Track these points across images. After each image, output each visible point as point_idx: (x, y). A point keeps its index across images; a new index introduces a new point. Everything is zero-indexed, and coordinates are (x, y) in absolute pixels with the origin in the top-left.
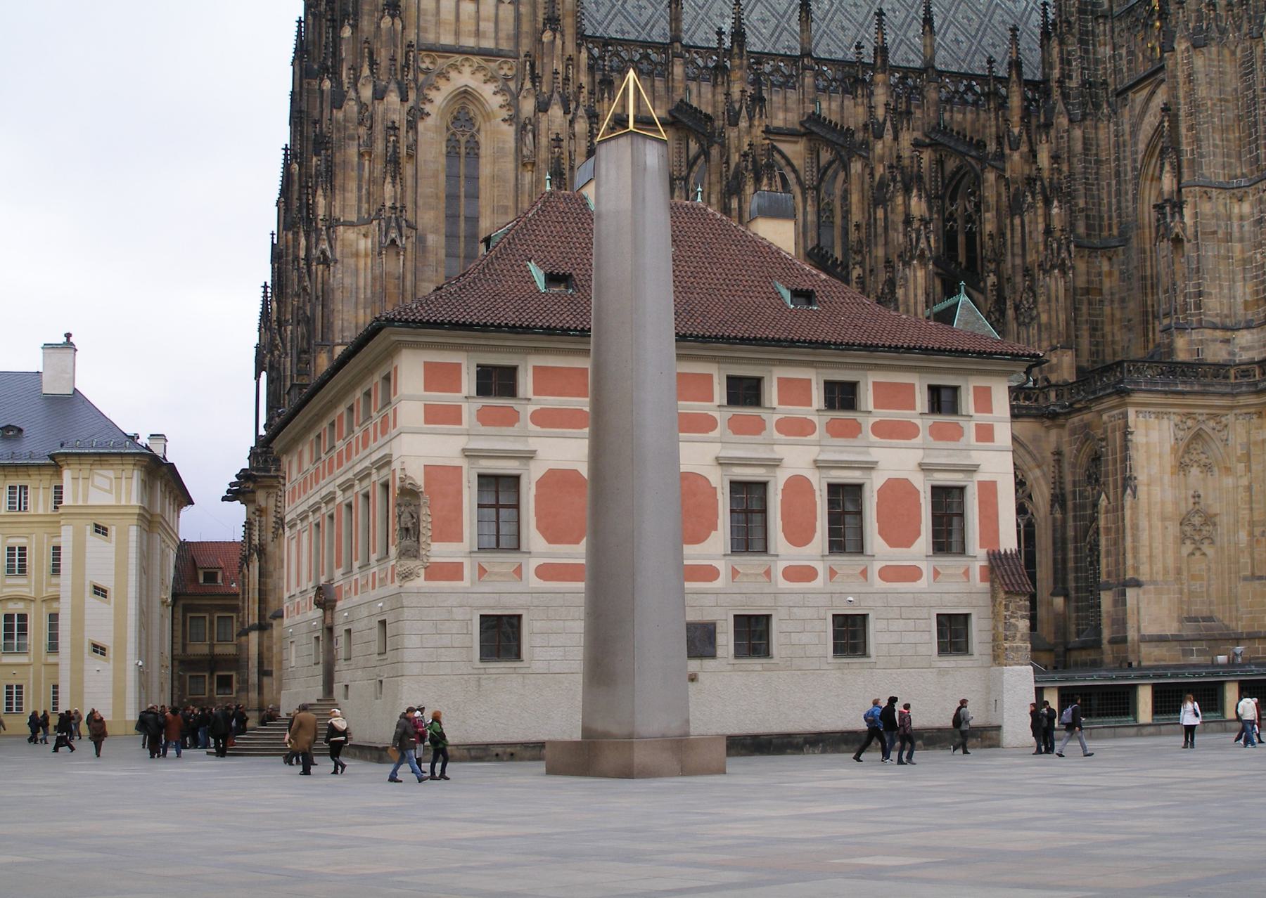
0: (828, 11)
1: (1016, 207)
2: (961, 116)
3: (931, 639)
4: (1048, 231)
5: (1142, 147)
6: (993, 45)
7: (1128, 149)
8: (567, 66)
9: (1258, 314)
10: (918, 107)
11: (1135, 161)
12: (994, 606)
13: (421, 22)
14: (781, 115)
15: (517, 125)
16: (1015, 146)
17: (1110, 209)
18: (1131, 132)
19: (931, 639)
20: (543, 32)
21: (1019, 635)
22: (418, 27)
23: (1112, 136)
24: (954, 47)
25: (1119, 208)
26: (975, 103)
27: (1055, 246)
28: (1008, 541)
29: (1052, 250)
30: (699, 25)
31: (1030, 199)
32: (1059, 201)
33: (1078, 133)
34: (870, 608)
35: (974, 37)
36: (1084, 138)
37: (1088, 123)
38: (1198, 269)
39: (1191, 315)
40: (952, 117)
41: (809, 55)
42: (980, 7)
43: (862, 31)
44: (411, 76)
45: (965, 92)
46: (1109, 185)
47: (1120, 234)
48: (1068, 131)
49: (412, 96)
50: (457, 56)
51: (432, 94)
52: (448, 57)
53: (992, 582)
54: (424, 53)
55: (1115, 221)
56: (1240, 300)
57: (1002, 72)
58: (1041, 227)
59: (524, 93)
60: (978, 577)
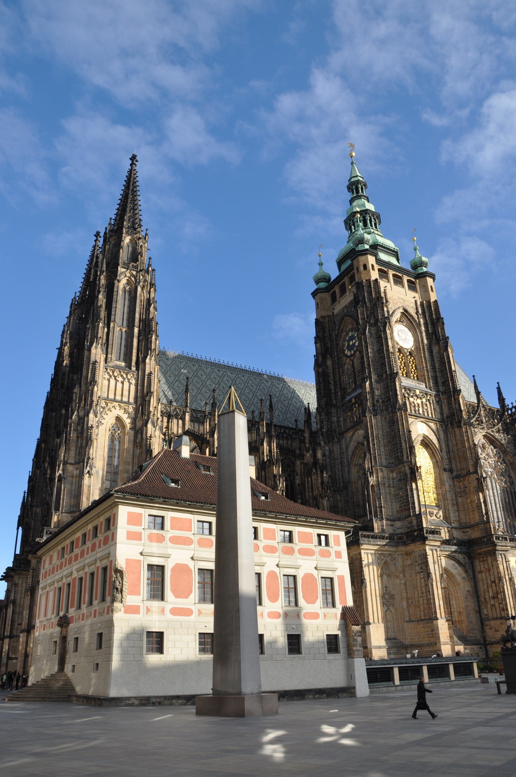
1: (309, 474)
2: (282, 442)
3: (324, 645)
4: (322, 483)
5: (350, 453)
6: (291, 418)
7: (345, 454)
8: (154, 411)
9: (403, 515)
11: (348, 459)
15: (135, 431)
16: (308, 451)
18: (346, 448)
19: (324, 645)
20: (147, 396)
25: (342, 476)
26: (287, 437)
27: (326, 488)
28: (350, 603)
29: (325, 489)
30: (193, 402)
31: (314, 471)
32: (326, 472)
33: (327, 448)
35: (284, 414)
36: (329, 450)
37: (330, 444)
42: (285, 404)
43: (248, 409)
45: (284, 433)
46: (338, 467)
48: (324, 447)
49: (99, 415)
50: (115, 403)
51: (105, 416)
52: (112, 403)
54: (103, 401)
55: (341, 481)
56: (395, 510)
57: (301, 426)
58: (320, 481)
59: (138, 419)
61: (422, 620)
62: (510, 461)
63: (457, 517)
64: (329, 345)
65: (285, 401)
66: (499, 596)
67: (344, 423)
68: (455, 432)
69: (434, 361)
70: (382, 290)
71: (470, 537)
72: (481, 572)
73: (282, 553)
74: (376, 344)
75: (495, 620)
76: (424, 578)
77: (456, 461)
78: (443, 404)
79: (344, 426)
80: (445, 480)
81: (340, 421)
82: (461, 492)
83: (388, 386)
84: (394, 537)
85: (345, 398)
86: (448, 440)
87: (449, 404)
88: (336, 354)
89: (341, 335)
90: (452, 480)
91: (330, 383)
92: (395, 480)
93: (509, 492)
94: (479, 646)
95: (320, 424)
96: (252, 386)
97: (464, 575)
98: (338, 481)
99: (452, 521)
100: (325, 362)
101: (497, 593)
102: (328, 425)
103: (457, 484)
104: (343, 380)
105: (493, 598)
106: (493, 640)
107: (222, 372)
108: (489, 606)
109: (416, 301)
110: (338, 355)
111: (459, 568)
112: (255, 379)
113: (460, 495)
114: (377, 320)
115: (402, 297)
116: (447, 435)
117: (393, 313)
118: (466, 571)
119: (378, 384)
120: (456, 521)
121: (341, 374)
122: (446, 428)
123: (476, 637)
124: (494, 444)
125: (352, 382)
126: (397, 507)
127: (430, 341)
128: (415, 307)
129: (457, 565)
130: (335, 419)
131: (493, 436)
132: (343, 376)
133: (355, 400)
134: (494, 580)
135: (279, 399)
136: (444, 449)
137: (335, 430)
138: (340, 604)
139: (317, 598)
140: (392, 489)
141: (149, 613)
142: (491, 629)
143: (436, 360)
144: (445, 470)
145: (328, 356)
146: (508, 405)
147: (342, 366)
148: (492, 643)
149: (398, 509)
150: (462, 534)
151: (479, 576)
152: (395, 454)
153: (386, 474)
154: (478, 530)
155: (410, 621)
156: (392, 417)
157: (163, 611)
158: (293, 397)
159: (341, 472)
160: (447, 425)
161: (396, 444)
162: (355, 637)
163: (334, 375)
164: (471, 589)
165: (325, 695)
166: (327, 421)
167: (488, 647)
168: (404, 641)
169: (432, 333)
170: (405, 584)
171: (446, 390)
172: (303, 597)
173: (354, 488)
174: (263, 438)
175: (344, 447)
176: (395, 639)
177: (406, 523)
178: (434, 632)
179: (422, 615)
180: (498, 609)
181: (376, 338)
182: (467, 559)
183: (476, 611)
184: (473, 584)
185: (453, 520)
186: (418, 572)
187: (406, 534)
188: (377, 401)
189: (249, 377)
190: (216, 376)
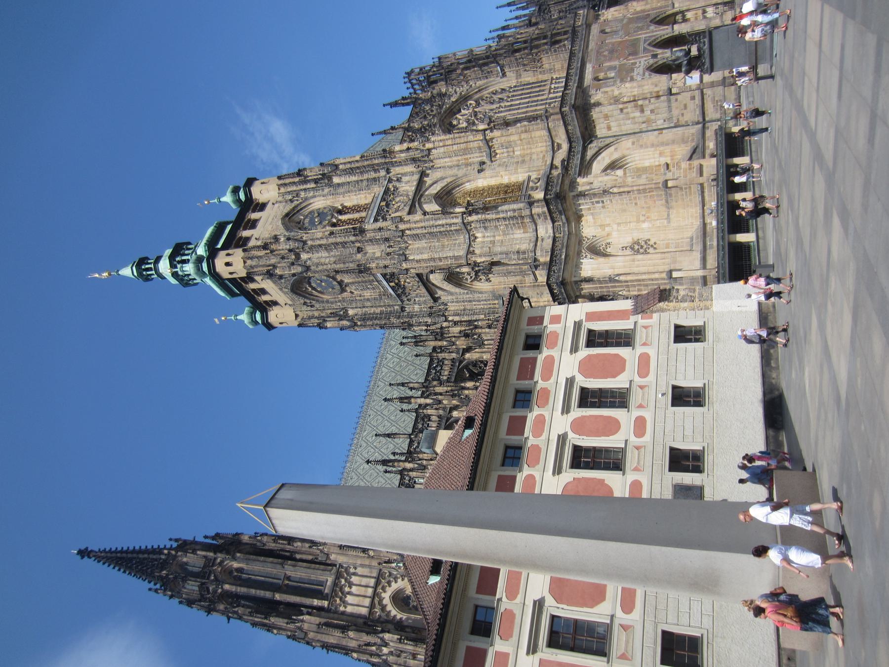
0: (396, 427)
11: (464, 293)
12: (669, 310)
17: (485, 304)
23: (453, 304)
24: (418, 375)
25: (485, 300)
34: (667, 383)
37: (446, 314)
38: (507, 254)
39: (528, 256)
40: (446, 375)
41: (410, 435)
46: (475, 305)
47: (498, 299)
53: (652, 312)
56: (523, 235)
61: (667, 202)
62: (476, 92)
64: (330, 311)
65: (401, 366)
66: (640, 103)
67: (421, 296)
68: (434, 159)
69: (348, 182)
71: (564, 141)
72: (609, 128)
73: (546, 407)
74: (320, 255)
75: (671, 109)
76: (611, 201)
77: (470, 158)
78: (401, 172)
79: (424, 296)
81: (418, 301)
82: (508, 152)
83: (371, 240)
84: (557, 238)
85: (391, 294)
87: (399, 164)
88: (339, 304)
89: (317, 296)
91: (374, 313)
92: (486, 235)
95: (422, 326)
96: (382, 405)
97: (612, 149)
98: (492, 306)
101: (636, 106)
102: (423, 316)
103: (498, 156)
104: (370, 296)
105: (642, 111)
106: (698, 112)
107: (363, 442)
108: (653, 117)
110: (340, 301)
111: (603, 155)
112: (373, 401)
113: (512, 154)
114: (290, 250)
115: (270, 220)
116: (438, 168)
118: (607, 146)
119: (367, 253)
121: (362, 298)
122: (430, 169)
123: (693, 135)
124: (455, 110)
125: (370, 284)
126: (520, 233)
127: (325, 186)
128: (284, 204)
129: (599, 158)
130: (417, 308)
131: (445, 112)
132: (364, 296)
133: (392, 282)
134: (619, 111)
135: (399, 373)
136: (455, 171)
137: (430, 308)
138: (628, 319)
139: (617, 355)
140: (497, 238)
141: (629, 655)
142: (683, 115)
143: (348, 180)
144: (480, 171)
145: (342, 313)
146: (410, 93)
147: (352, 297)
149: (522, 231)
150: (560, 151)
151: (615, 130)
152: (453, 234)
153: (478, 246)
154: (555, 131)
155: (668, 218)
156: (407, 236)
157: (625, 628)
158: (398, 355)
159: (480, 302)
160: (426, 167)
161: (440, 232)
163: (364, 307)
164: (630, 141)
166: (418, 318)
168: (695, 227)
170: (619, 224)
171: (384, 168)
172: (614, 376)
173: (500, 286)
174: (432, 401)
175: (450, 297)
176: (692, 238)
177: (539, 222)
178: (683, 187)
179: (660, 202)
180: (657, 105)
181: (313, 254)
183: (659, 134)
184: (624, 138)
185: (543, 162)
186: (603, 207)
187: (553, 221)
188: (388, 254)
189: (371, 409)
190: (367, 451)
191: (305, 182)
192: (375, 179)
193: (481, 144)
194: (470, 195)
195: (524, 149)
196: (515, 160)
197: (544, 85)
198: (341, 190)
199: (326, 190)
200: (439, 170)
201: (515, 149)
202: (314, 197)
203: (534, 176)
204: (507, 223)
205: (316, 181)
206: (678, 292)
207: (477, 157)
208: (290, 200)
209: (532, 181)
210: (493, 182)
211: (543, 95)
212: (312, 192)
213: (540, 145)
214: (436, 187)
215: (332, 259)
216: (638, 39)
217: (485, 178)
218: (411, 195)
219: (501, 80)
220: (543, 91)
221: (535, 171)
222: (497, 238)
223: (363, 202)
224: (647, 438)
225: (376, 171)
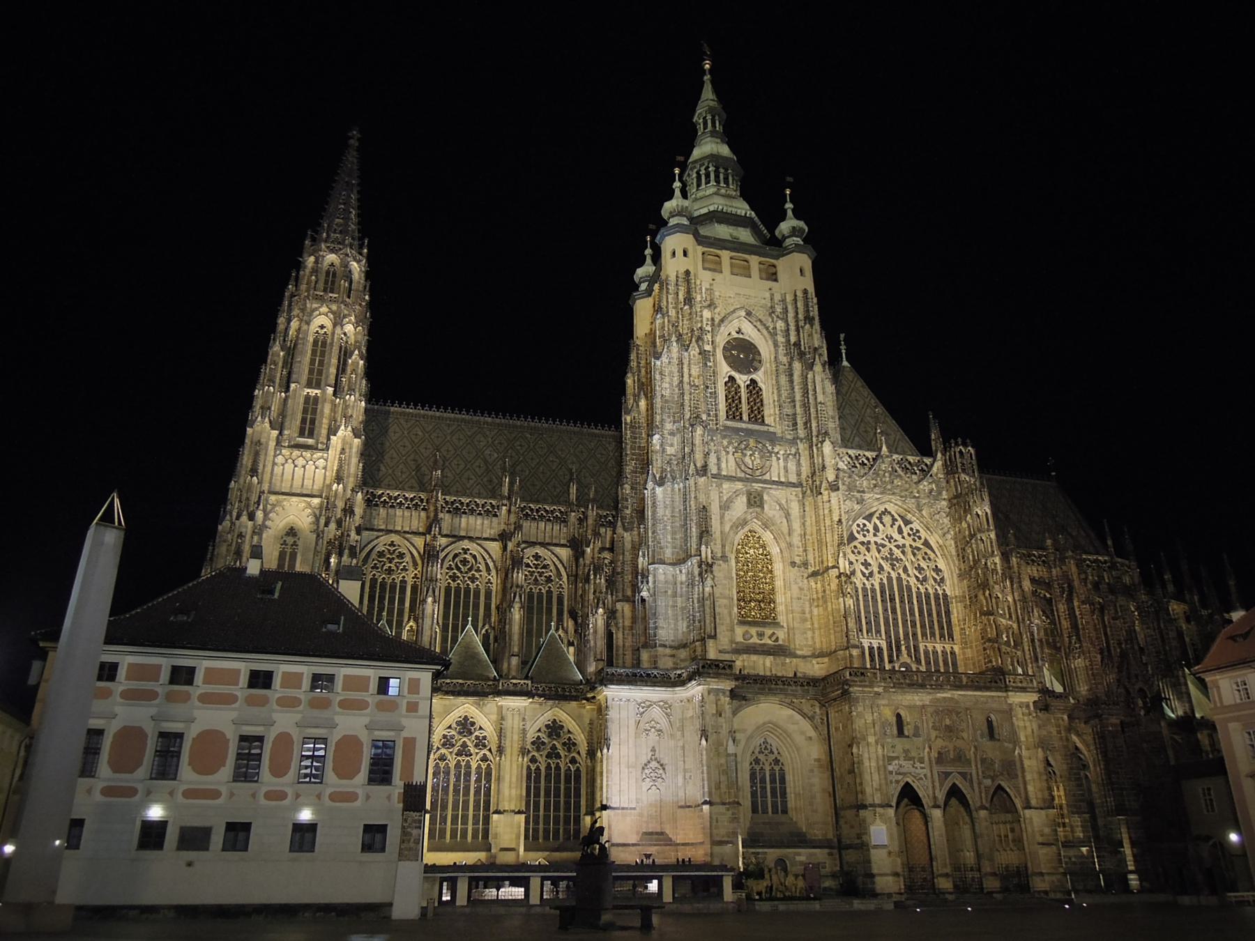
10: (565, 526)
13: (273, 481)
14: (488, 531)
21: (412, 840)
22: (270, 483)
38: (655, 613)
44: (261, 507)
56: (680, 632)
60: (396, 800)
63: (810, 639)
69: (793, 389)
70: (705, 286)
78: (802, 458)
80: (792, 580)
82: (818, 599)
86: (804, 517)
87: (812, 457)
90: (806, 581)
93: (932, 596)
94: (826, 851)
97: (812, 733)
99: (797, 647)
100: (638, 406)
106: (848, 842)
109: (772, 295)
113: (816, 604)
117: (722, 321)
118: (816, 728)
120: (805, 646)
127: (792, 358)
128: (769, 305)
140: (679, 599)
142: (846, 823)
143: (797, 388)
144: (793, 564)
148: (849, 847)
149: (685, 630)
162: (409, 830)
164: (823, 757)
165: (333, 914)
167: (843, 852)
169: (794, 345)
170: (683, 747)
182: (817, 710)
183: (829, 793)
191: (798, 330)
192: (795, 424)
193: (825, 565)
194: (762, 554)
195: (819, 620)
196: (807, 610)
197: (942, 636)
198: (784, 380)
199: (784, 360)
200: (802, 510)
201: (821, 609)
202: (776, 345)
203: (781, 634)
204: (691, 613)
205: (797, 344)
206: (416, 827)
207: (815, 558)
208: (773, 312)
209: (774, 633)
210: (779, 583)
211: (924, 634)
212: (783, 340)
213: (824, 640)
214: (775, 510)
215: (667, 393)
216: (970, 763)
217: (784, 572)
218: (767, 477)
219: (955, 575)
220: (933, 634)
221: (789, 635)
222: (679, 599)
223: (766, 413)
224: (263, 801)
225: (805, 424)
